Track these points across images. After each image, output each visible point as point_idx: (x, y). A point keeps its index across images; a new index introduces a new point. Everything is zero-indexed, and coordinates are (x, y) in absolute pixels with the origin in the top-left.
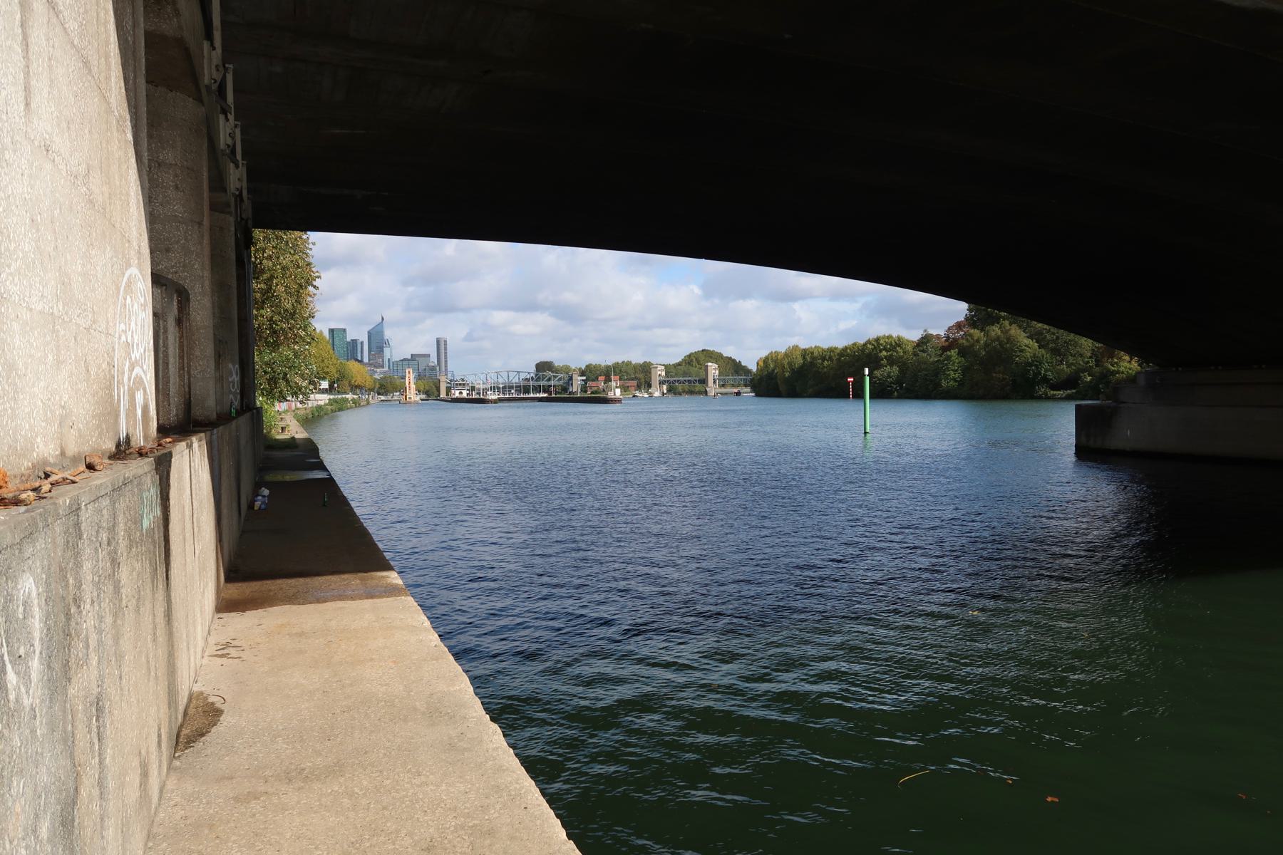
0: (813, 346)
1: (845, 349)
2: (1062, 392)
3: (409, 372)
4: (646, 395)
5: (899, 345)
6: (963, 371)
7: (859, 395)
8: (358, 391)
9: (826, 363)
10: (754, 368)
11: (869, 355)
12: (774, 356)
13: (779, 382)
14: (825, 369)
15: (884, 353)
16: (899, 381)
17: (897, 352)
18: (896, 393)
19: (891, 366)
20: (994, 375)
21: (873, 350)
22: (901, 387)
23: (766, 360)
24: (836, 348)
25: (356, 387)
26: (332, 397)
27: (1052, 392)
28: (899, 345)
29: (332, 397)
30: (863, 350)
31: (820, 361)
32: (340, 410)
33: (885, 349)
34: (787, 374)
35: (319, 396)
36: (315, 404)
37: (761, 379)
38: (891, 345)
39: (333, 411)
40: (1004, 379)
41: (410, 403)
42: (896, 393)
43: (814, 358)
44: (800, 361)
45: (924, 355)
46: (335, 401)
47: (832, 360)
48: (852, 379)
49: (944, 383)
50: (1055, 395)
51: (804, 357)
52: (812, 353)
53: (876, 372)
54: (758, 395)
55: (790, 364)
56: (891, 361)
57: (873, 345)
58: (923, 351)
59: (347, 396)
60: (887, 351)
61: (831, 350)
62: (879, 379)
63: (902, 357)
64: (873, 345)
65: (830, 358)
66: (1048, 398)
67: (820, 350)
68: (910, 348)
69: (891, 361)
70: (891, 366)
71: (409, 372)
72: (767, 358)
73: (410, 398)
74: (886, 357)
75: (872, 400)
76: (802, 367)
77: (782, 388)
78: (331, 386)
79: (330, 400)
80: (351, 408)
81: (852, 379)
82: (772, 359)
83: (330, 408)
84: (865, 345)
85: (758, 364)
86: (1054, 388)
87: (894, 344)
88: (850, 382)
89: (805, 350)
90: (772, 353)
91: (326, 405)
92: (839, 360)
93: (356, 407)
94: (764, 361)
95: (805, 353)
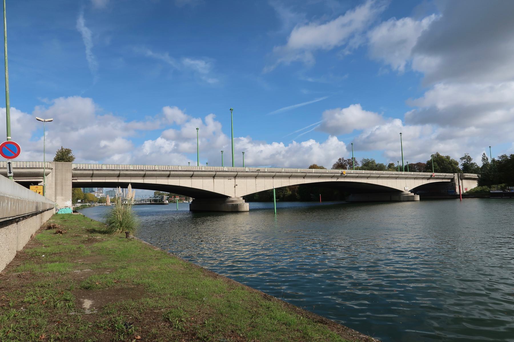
3: (108, 196)
4: (187, 202)
8: (91, 202)
25: (90, 201)
26: (82, 204)
29: (82, 204)
32: (84, 208)
35: (77, 204)
36: (77, 206)
39: (81, 208)
41: (108, 206)
46: (83, 205)
59: (87, 204)
71: (108, 196)
73: (108, 204)
78: (82, 201)
79: (81, 205)
80: (88, 207)
83: (81, 207)
91: (80, 206)
93: (89, 207)
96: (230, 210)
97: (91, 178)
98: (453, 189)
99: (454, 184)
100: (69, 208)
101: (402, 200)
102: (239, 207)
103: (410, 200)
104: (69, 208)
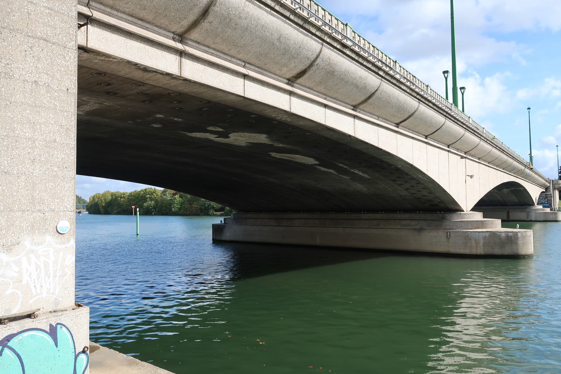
0: (117, 192)
1: (131, 194)
2: (219, 213)
5: (154, 193)
6: (181, 205)
7: (136, 214)
9: (122, 199)
10: (88, 201)
11: (142, 196)
12: (97, 195)
13: (100, 208)
14: (122, 202)
15: (148, 196)
16: (155, 208)
17: (154, 195)
18: (153, 213)
19: (151, 201)
20: (193, 205)
21: (144, 194)
22: (155, 210)
23: (94, 198)
24: (126, 193)
27: (215, 213)
28: (154, 193)
30: (139, 194)
31: (119, 198)
33: (149, 194)
34: (104, 204)
37: (91, 206)
38: (151, 192)
40: (197, 207)
42: (153, 213)
43: (117, 198)
44: (110, 198)
45: (165, 197)
47: (125, 198)
48: (134, 207)
49: (173, 209)
50: (216, 214)
51: (112, 196)
52: (116, 195)
53: (144, 204)
54: (90, 213)
55: (105, 200)
56: (151, 199)
57: (144, 192)
58: (165, 195)
60: (150, 195)
61: (124, 194)
62: (146, 207)
63: (155, 198)
64: (144, 192)
65: (124, 197)
66: (214, 215)
67: (119, 193)
68: (159, 194)
69: (151, 199)
70: (151, 201)
72: (94, 196)
74: (149, 197)
75: (140, 216)
76: (111, 201)
77: (102, 210)
81: (134, 207)
82: (97, 197)
84: (139, 192)
85: (90, 199)
86: (216, 211)
87: (152, 192)
88: (133, 208)
89: (112, 193)
90: (96, 194)
92: (128, 198)
94: (93, 198)
95: (112, 194)
96: (480, 251)
97: (179, 46)
98: (547, 202)
99: (550, 196)
100: (53, 332)
101: (533, 219)
102: (520, 242)
103: (550, 219)
104: (53, 332)
